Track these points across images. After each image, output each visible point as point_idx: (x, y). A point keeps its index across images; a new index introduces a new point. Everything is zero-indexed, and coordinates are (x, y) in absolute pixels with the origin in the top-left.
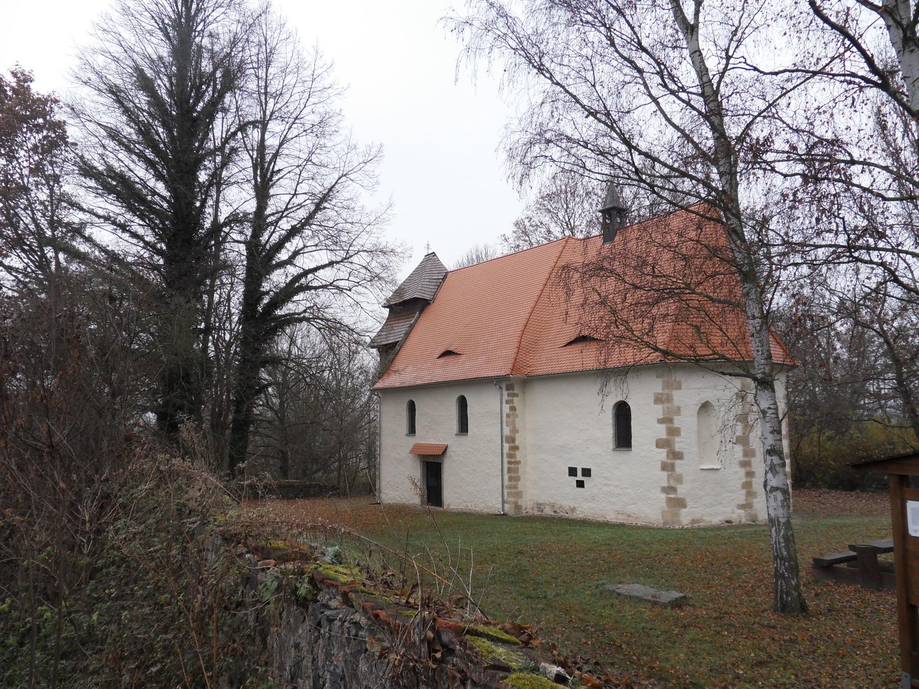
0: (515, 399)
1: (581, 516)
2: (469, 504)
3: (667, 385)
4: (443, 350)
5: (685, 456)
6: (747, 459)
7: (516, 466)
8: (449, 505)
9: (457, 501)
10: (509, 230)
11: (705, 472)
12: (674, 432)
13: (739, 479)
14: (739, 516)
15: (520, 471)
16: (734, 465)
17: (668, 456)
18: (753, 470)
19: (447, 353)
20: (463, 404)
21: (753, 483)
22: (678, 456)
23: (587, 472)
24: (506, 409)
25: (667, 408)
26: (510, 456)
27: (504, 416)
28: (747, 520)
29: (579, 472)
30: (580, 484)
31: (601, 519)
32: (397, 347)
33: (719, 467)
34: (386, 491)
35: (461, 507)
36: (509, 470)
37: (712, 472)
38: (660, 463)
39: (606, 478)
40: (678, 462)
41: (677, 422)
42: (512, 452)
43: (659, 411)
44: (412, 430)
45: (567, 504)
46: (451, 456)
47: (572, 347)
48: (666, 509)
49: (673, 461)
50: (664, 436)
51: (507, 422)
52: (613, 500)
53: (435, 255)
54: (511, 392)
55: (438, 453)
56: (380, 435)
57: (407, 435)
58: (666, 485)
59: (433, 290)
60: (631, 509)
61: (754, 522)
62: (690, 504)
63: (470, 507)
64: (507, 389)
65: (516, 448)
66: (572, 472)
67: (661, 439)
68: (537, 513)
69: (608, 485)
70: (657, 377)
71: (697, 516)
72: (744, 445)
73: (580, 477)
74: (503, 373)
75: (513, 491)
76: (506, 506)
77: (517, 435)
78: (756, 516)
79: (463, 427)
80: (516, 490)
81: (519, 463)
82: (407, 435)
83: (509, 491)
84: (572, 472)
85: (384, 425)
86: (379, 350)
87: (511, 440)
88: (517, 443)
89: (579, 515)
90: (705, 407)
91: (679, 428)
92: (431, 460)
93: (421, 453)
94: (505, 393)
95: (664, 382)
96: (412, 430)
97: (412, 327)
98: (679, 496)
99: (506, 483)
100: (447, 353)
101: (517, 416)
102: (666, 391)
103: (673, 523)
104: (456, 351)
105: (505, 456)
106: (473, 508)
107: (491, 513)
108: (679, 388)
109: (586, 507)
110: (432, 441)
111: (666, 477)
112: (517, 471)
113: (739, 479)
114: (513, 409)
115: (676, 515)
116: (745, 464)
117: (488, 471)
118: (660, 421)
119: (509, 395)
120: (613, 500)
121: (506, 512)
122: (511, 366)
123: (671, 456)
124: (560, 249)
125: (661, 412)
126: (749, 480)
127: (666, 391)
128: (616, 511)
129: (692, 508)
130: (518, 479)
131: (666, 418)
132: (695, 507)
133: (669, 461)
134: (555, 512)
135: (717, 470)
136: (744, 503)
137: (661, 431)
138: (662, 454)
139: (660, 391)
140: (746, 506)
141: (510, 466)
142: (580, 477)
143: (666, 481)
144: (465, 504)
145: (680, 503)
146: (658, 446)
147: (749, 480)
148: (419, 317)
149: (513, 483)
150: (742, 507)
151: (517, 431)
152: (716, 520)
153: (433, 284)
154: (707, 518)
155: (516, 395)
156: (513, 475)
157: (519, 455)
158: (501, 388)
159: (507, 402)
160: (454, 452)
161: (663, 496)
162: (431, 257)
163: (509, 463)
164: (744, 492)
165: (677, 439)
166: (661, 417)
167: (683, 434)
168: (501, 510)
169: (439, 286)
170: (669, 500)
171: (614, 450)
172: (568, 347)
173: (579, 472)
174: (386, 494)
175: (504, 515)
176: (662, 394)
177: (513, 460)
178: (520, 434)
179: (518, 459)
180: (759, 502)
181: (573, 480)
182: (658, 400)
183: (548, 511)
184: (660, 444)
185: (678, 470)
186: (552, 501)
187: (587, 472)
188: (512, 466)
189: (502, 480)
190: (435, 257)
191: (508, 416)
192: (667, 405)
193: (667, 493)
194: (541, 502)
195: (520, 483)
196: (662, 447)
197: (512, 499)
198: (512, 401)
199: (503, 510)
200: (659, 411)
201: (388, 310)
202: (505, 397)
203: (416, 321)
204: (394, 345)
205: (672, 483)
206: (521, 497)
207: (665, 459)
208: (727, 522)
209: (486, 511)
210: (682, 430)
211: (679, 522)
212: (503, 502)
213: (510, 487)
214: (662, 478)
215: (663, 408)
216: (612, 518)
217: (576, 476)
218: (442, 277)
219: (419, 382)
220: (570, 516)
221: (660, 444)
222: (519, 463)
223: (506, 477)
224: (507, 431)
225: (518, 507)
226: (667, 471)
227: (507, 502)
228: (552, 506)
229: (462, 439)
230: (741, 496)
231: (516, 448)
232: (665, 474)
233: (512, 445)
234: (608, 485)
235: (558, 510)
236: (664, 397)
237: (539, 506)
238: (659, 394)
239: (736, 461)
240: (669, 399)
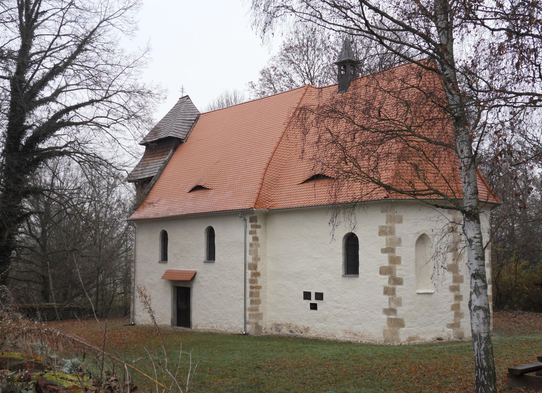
0: (258, 230)
1: (314, 335)
2: (215, 325)
3: (391, 219)
4: (193, 185)
5: (404, 283)
6: (456, 284)
7: (257, 290)
8: (196, 326)
9: (204, 322)
10: (256, 78)
11: (420, 296)
12: (395, 260)
13: (449, 302)
14: (448, 334)
15: (261, 295)
16: (445, 290)
17: (389, 282)
18: (461, 294)
19: (198, 188)
20: (211, 234)
21: (461, 305)
22: (398, 281)
23: (319, 296)
24: (250, 238)
25: (390, 239)
26: (252, 281)
27: (248, 245)
28: (455, 337)
29: (313, 296)
30: (314, 307)
31: (331, 338)
32: (152, 182)
33: (433, 291)
34: (140, 314)
35: (207, 328)
36: (251, 294)
37: (426, 295)
38: (383, 288)
39: (336, 301)
40: (398, 287)
41: (399, 252)
42: (254, 278)
43: (383, 242)
44: (164, 258)
45: (302, 324)
46: (199, 282)
47: (308, 184)
48: (387, 328)
49: (394, 286)
50: (386, 264)
51: (250, 251)
52: (342, 320)
53: (189, 98)
54: (254, 223)
55: (187, 279)
56: (134, 262)
57: (159, 262)
58: (387, 307)
59: (186, 130)
60: (357, 328)
61: (460, 339)
62: (407, 324)
63: (215, 328)
64: (251, 220)
65: (257, 274)
66: (307, 296)
67: (384, 267)
68: (275, 333)
69: (338, 308)
70: (382, 212)
71: (414, 334)
72: (453, 273)
73: (313, 300)
74: (247, 207)
75: (254, 313)
76: (248, 326)
77: (259, 262)
78: (462, 334)
79: (211, 256)
80: (257, 312)
81: (260, 287)
82: (159, 262)
83: (251, 313)
84: (307, 296)
85: (138, 253)
86: (136, 184)
87: (254, 267)
88: (259, 270)
89: (312, 334)
90: (422, 238)
91: (400, 257)
92: (181, 285)
93: (174, 279)
94: (249, 224)
95: (387, 216)
96: (164, 258)
97: (166, 163)
98: (399, 317)
99: (248, 305)
100: (198, 188)
101: (259, 245)
102: (389, 224)
103: (393, 340)
104: (206, 186)
105: (248, 281)
106: (219, 328)
107: (234, 333)
108: (400, 221)
109: (318, 327)
110: (182, 268)
111: (387, 301)
112: (258, 294)
113: (449, 302)
114: (256, 239)
115: (396, 333)
116: (454, 289)
117: (232, 295)
118: (384, 251)
119: (252, 226)
120: (342, 320)
121: (248, 332)
122: (254, 201)
123: (392, 282)
124: (301, 96)
125: (385, 243)
126: (457, 302)
127: (389, 224)
128: (344, 331)
129: (408, 327)
130: (258, 302)
131: (389, 248)
132: (411, 327)
133: (391, 286)
134: (291, 331)
135: (431, 294)
136: (453, 322)
137: (384, 260)
138: (385, 280)
139: (384, 224)
140: (455, 325)
141: (252, 290)
142: (313, 300)
143: (388, 304)
144: (211, 325)
145: (400, 323)
146: (382, 273)
147: (457, 302)
148: (172, 155)
149: (254, 306)
150: (451, 326)
151: (259, 259)
152: (429, 338)
153: (187, 124)
154: (422, 336)
155: (259, 227)
156: (254, 298)
157: (260, 281)
158: (245, 220)
159: (251, 233)
160: (202, 278)
161: (385, 317)
162: (185, 100)
163: (251, 288)
164: (453, 313)
165: (398, 267)
166: (385, 247)
167: (402, 262)
168: (243, 330)
169: (192, 127)
170: (389, 320)
171: (343, 276)
172: (306, 184)
173: (313, 296)
174: (139, 316)
175: (246, 334)
176: (386, 227)
177: (254, 285)
178: (261, 261)
179: (259, 284)
180: (465, 322)
181: (307, 303)
182: (382, 232)
183: (285, 331)
184: (383, 271)
185: (398, 294)
186: (289, 322)
187: (319, 296)
188: (254, 290)
189: (245, 303)
190: (188, 100)
191: (251, 245)
192: (389, 237)
193: (388, 315)
194: (279, 323)
195: (260, 305)
196: (385, 274)
197: (253, 320)
198: (255, 232)
199: (245, 330)
200: (383, 242)
201: (145, 147)
202: (249, 229)
203: (170, 158)
204: (149, 179)
205: (393, 306)
206: (261, 319)
207: (387, 285)
208: (439, 339)
209: (230, 331)
210: (402, 259)
211: (398, 340)
212: (246, 323)
213: (251, 310)
214: (384, 301)
215: (387, 239)
216: (340, 336)
217: (310, 299)
218: (195, 119)
219: (171, 214)
220: (304, 335)
221: (383, 271)
222: (260, 287)
223: (248, 300)
224: (250, 259)
225: (258, 327)
226: (389, 295)
227: (249, 323)
228: (289, 326)
229: (210, 266)
230: (450, 317)
231: (257, 274)
232: (386, 297)
233: (254, 271)
234: (338, 308)
235: (293, 330)
236: (388, 230)
237: (277, 326)
238: (383, 227)
239: (447, 286)
240: (392, 232)
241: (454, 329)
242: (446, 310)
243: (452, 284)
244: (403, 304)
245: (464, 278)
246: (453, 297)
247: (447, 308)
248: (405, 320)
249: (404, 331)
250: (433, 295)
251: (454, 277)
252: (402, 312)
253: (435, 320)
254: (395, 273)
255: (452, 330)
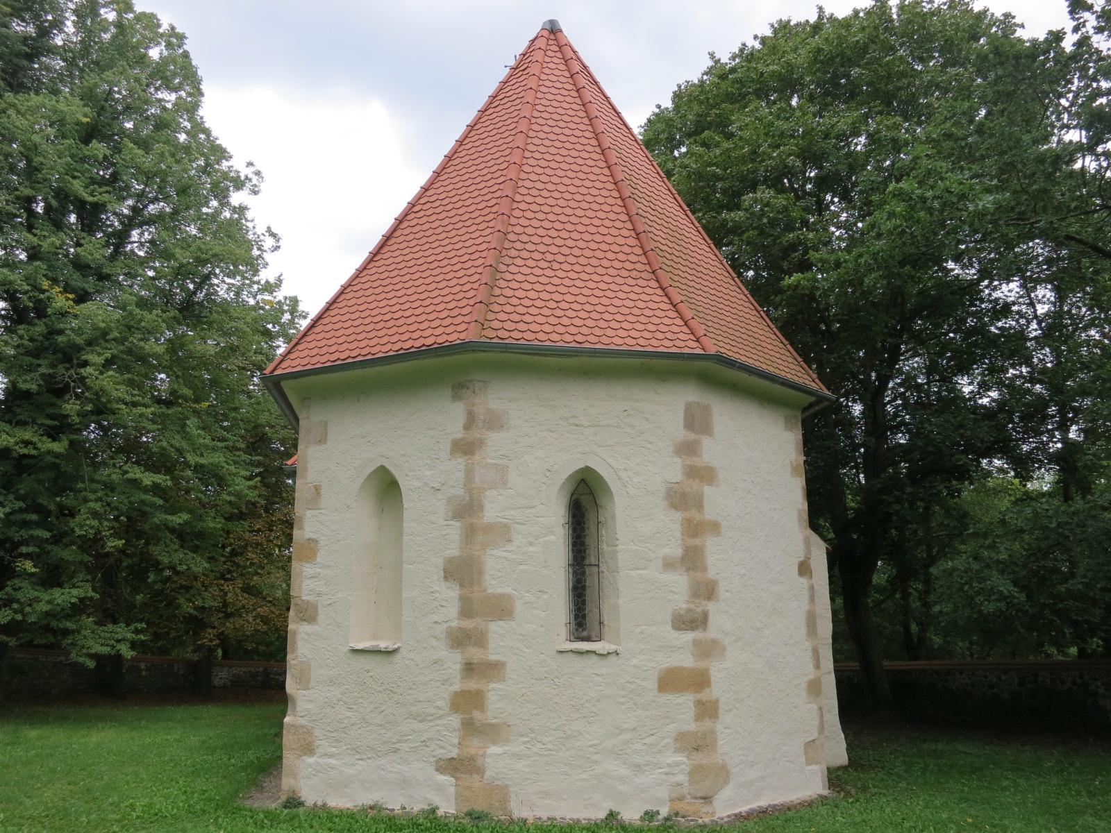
5: (321, 617)
6: (468, 624)
11: (361, 659)
16: (433, 642)
18: (493, 658)
37: (378, 658)
62: (323, 745)
72: (462, 585)
98: (301, 721)
132: (331, 756)
136: (454, 753)
164: (455, 720)
239: (440, 630)
241: (457, 779)
242: (433, 710)
243: (454, 624)
244: (312, 684)
245: (518, 603)
246: (458, 667)
247: (438, 703)
248: (317, 733)
249: (311, 765)
250: (398, 657)
251: (461, 598)
252: (309, 706)
253: (399, 741)
254: (300, 587)
255: (452, 780)
